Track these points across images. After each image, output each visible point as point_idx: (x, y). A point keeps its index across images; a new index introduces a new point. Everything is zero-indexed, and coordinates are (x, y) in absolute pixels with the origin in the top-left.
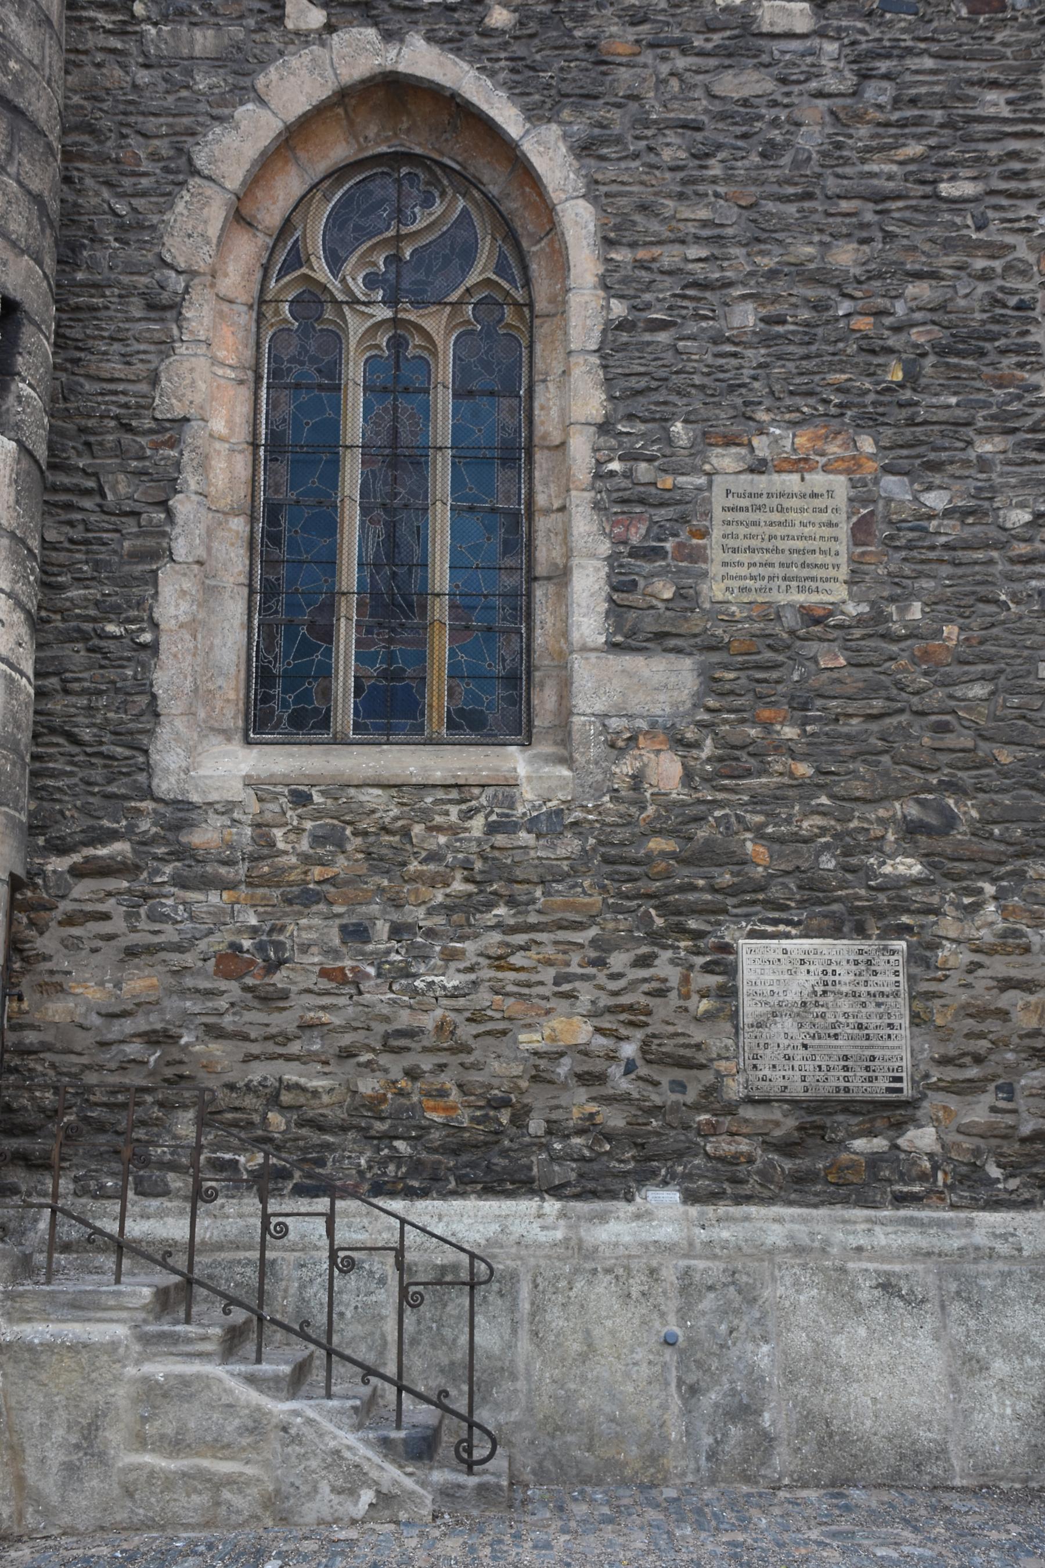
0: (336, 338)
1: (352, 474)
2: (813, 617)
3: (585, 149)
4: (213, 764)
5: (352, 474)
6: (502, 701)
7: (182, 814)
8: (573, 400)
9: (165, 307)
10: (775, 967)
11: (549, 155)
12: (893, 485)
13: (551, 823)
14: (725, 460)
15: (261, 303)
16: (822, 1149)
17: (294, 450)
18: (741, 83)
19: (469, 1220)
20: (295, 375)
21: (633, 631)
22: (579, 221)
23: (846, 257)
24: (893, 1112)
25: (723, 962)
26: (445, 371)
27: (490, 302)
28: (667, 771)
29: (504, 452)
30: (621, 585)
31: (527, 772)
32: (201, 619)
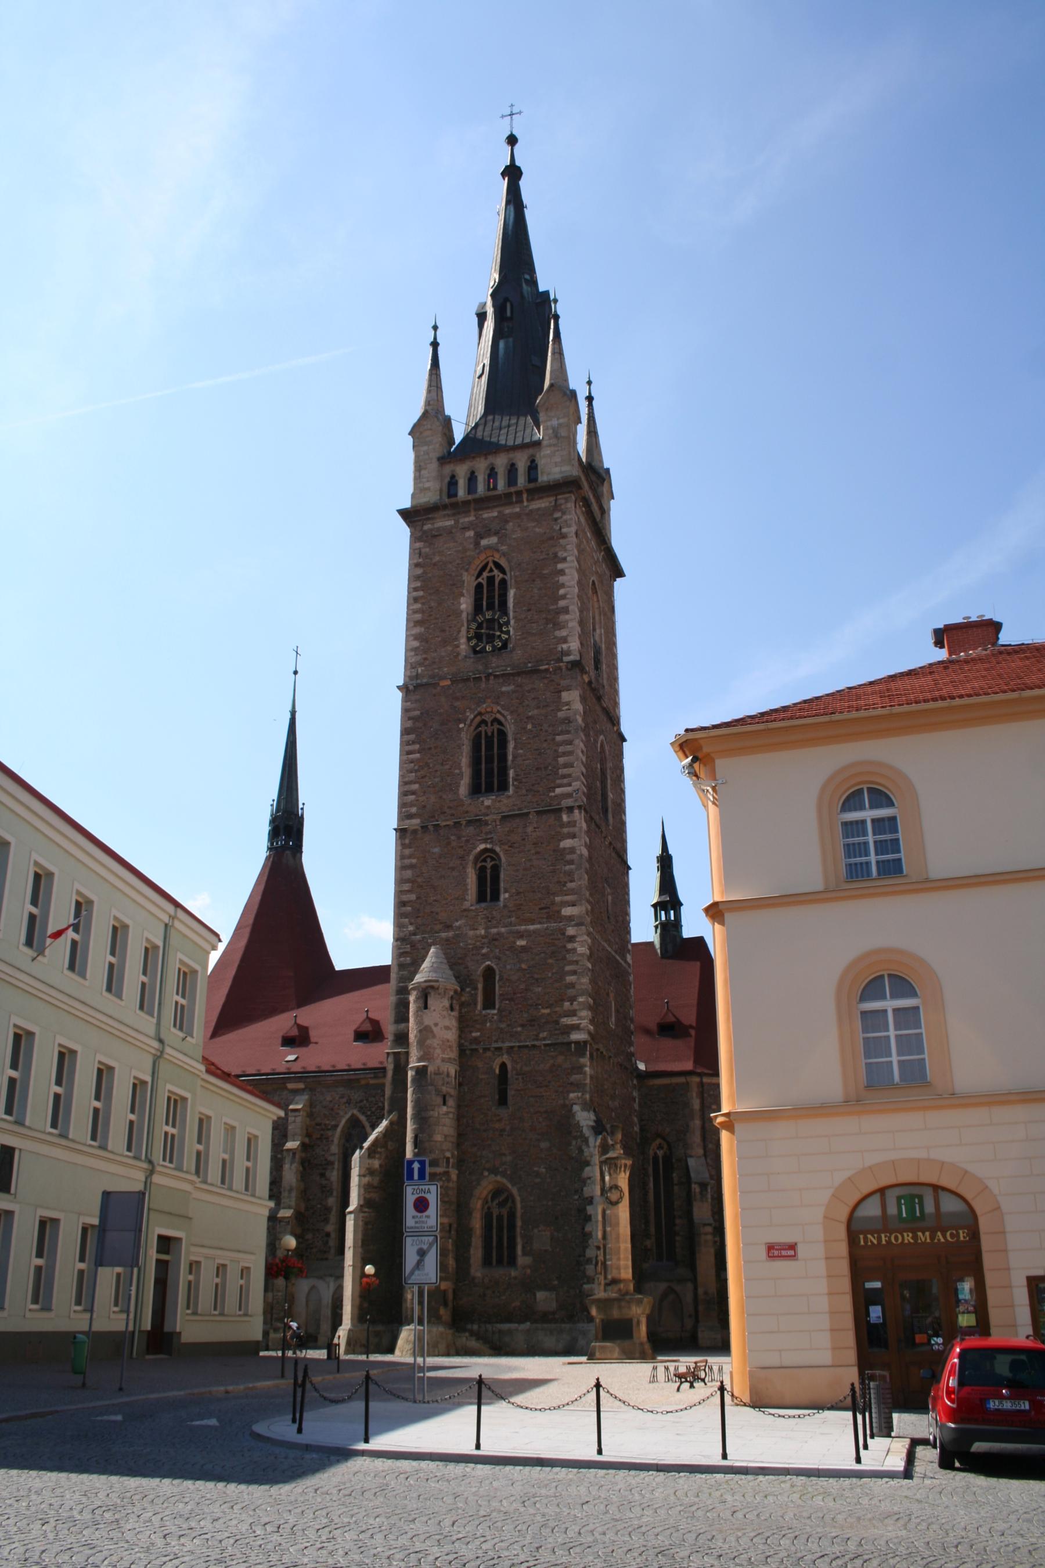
0: (492, 1213)
1: (494, 1231)
2: (546, 1251)
3: (519, 1190)
4: (477, 1271)
5: (494, 1231)
6: (512, 1261)
7: (474, 1278)
8: (519, 1223)
9: (470, 1214)
10: (540, 1295)
11: (515, 1191)
12: (555, 1234)
13: (515, 1278)
14: (536, 1231)
15: (483, 1208)
16: (545, 1318)
17: (487, 1227)
18: (538, 1180)
19: (506, 1326)
20: (488, 1217)
21: (524, 1254)
22: (518, 1199)
23: (550, 1203)
24: (554, 1313)
25: (535, 1295)
26: (505, 1217)
27: (511, 1208)
28: (529, 1271)
29: (512, 1227)
30: (523, 1247)
31: (513, 1273)
32: (476, 1253)
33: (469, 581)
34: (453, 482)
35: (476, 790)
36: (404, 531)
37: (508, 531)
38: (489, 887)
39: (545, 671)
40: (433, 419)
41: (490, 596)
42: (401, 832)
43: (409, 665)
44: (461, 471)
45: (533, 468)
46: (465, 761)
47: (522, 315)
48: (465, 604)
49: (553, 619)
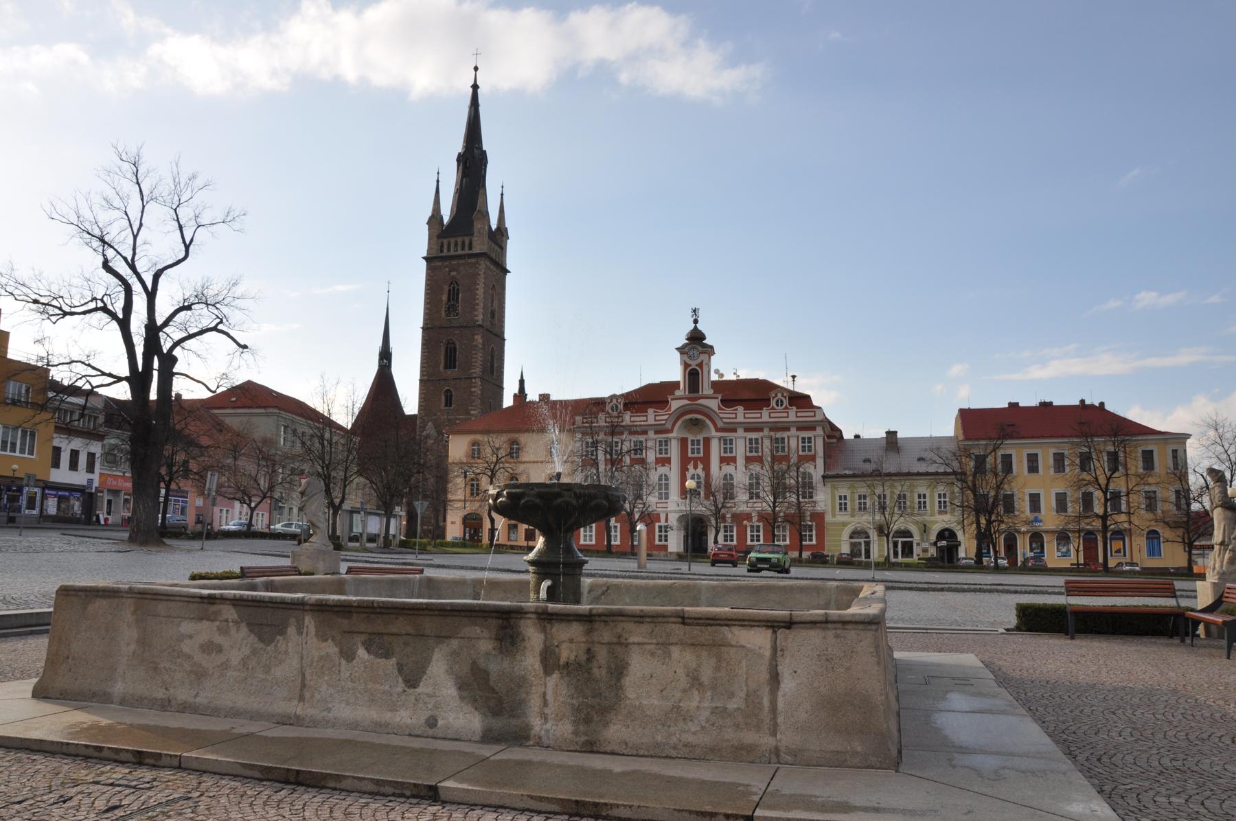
33: (446, 288)
34: (442, 246)
35: (446, 367)
36: (424, 263)
37: (466, 259)
38: (448, 403)
39: (471, 327)
40: (435, 218)
41: (453, 295)
42: (421, 381)
43: (425, 320)
44: (445, 242)
45: (471, 244)
46: (442, 357)
47: (472, 163)
48: (445, 298)
49: (473, 307)
